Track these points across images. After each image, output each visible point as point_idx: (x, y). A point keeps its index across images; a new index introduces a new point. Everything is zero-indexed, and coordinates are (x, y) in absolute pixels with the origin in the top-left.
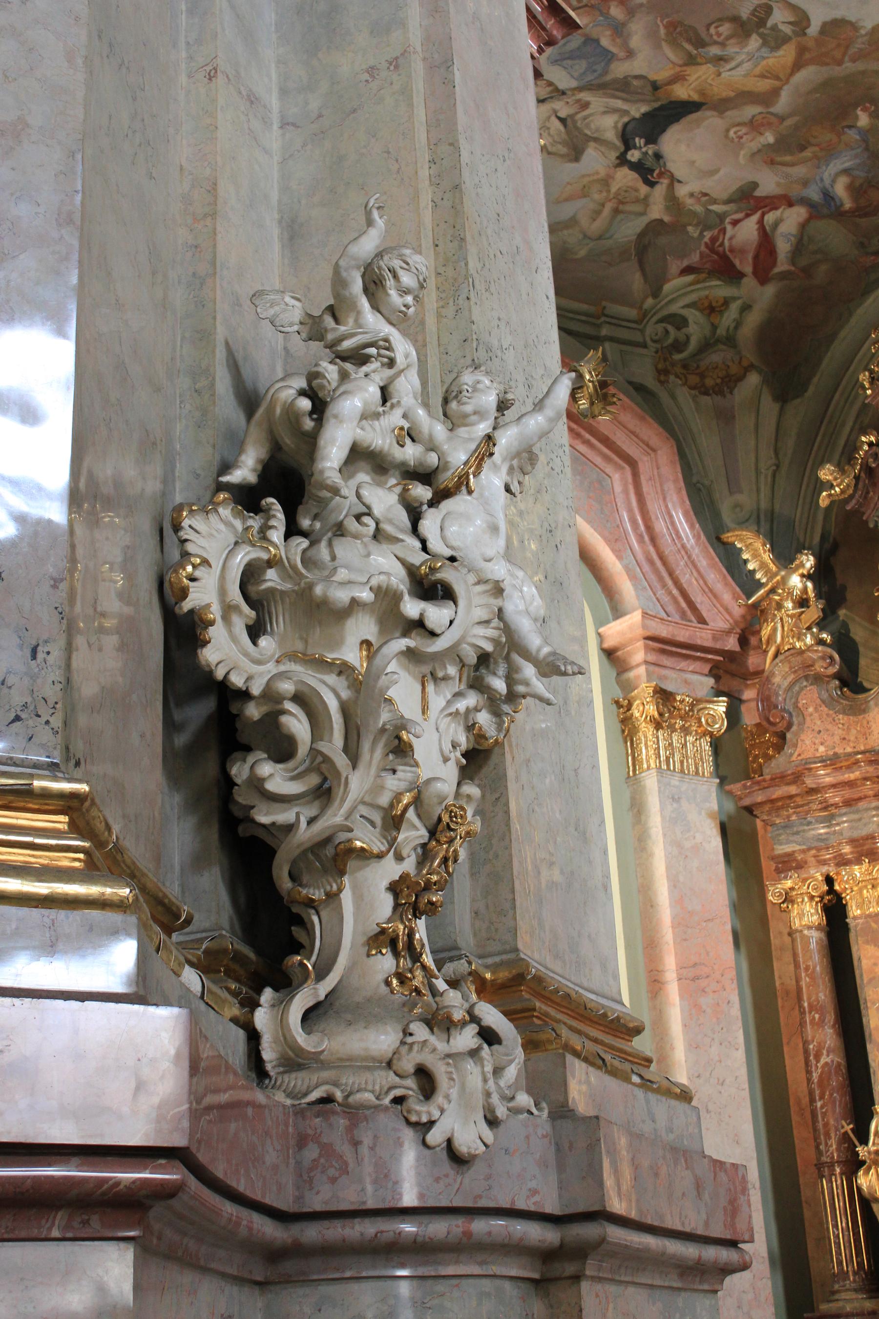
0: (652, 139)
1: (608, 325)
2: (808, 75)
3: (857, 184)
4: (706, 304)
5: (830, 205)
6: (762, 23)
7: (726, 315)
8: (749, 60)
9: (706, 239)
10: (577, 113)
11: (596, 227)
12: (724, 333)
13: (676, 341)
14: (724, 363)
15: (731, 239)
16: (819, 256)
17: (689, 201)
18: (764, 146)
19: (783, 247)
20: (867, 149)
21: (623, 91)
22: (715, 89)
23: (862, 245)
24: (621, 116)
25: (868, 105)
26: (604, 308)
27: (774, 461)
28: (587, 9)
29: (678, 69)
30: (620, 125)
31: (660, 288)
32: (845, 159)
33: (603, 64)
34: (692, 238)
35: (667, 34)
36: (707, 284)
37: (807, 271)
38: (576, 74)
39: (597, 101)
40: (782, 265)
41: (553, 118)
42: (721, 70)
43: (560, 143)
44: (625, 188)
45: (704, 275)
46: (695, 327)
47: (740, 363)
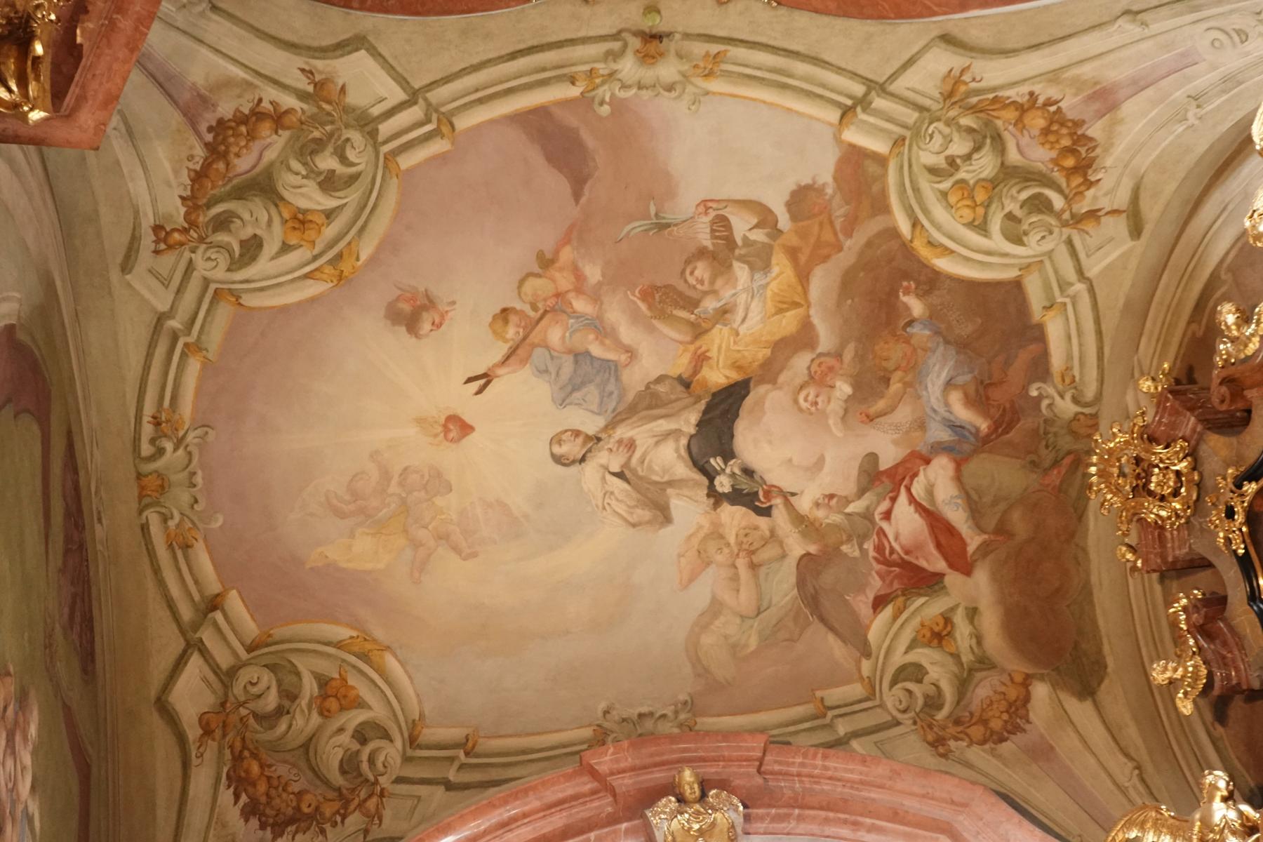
0: (728, 455)
1: (840, 720)
2: (822, 282)
3: (972, 390)
4: (928, 634)
5: (964, 436)
6: (730, 242)
7: (958, 635)
8: (752, 297)
9: (872, 553)
10: (630, 458)
11: (746, 598)
12: (971, 657)
13: (927, 697)
14: (995, 692)
15: (896, 538)
16: (1002, 506)
17: (820, 514)
18: (846, 401)
19: (957, 516)
20: (947, 342)
21: (657, 406)
22: (746, 354)
23: (1033, 463)
24: (677, 441)
25: (905, 284)
26: (822, 699)
27: (1130, 765)
28: (548, 316)
29: (692, 348)
30: (683, 452)
31: (866, 642)
32: (937, 368)
33: (613, 380)
34: (855, 558)
35: (650, 307)
36: (912, 608)
37: (1002, 530)
38: (594, 407)
39: (641, 433)
40: (974, 541)
41: (609, 477)
42: (735, 326)
43: (636, 506)
44: (742, 532)
45: (901, 599)
46: (936, 668)
47: (1012, 680)
